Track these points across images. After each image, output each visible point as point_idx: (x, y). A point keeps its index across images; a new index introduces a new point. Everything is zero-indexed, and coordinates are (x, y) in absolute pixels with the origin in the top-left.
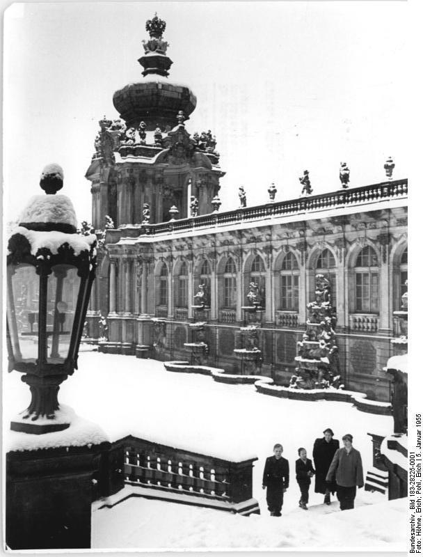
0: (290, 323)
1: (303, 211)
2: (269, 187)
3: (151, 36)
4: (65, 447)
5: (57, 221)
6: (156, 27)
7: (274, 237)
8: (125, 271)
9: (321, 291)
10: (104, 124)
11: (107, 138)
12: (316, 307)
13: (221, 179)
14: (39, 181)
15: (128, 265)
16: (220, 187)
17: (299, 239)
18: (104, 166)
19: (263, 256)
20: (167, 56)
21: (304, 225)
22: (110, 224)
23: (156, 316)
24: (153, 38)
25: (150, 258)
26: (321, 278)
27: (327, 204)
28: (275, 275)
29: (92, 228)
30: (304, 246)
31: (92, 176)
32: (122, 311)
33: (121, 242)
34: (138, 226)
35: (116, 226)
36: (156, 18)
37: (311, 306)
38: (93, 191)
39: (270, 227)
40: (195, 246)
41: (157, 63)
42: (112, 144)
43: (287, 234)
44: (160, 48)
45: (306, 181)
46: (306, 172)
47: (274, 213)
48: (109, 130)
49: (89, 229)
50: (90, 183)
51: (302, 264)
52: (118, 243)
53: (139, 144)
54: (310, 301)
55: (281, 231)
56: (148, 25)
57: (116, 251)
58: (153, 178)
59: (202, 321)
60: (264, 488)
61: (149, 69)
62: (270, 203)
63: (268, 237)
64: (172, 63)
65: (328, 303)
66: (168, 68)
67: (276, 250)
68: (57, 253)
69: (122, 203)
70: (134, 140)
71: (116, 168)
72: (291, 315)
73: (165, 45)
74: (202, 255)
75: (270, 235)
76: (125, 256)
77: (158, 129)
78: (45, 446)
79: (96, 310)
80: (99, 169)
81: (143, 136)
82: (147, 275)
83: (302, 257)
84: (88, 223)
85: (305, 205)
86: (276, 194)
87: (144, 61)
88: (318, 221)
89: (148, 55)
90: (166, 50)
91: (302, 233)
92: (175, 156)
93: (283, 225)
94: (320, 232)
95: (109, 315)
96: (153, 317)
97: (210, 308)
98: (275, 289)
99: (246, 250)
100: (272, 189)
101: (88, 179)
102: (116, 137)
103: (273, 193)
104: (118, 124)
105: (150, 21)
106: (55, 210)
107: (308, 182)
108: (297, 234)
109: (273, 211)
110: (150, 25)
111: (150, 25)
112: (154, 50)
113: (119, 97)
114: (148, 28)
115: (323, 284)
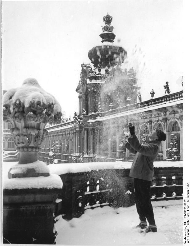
0: (160, 159)
1: (165, 102)
2: (150, 91)
3: (106, 24)
6: (108, 20)
7: (153, 116)
9: (173, 142)
10: (83, 66)
11: (84, 72)
12: (171, 151)
17: (163, 117)
18: (84, 86)
19: (148, 125)
20: (113, 33)
21: (165, 109)
22: (84, 113)
23: (103, 156)
24: (107, 25)
26: (173, 136)
27: (176, 98)
29: (78, 115)
30: (166, 120)
31: (78, 91)
32: (90, 153)
33: (89, 121)
34: (96, 114)
35: (87, 113)
37: (168, 150)
38: (80, 97)
39: (150, 111)
40: (120, 122)
41: (108, 36)
42: (86, 75)
43: (158, 114)
44: (109, 29)
45: (167, 87)
46: (167, 83)
47: (153, 104)
48: (85, 68)
49: (77, 115)
50: (78, 94)
51: (165, 129)
52: (88, 122)
53: (97, 75)
54: (168, 148)
55: (155, 113)
57: (87, 125)
59: (122, 158)
61: (104, 39)
62: (151, 99)
63: (150, 116)
64: (115, 36)
65: (176, 148)
66: (114, 39)
67: (154, 123)
69: (90, 102)
70: (96, 73)
71: (88, 86)
72: (160, 155)
73: (112, 28)
75: (151, 115)
76: (91, 128)
77: (107, 67)
79: (80, 153)
80: (82, 87)
81: (100, 71)
83: (165, 126)
84: (77, 113)
85: (166, 99)
86: (154, 95)
87: (102, 36)
88: (171, 107)
89: (104, 33)
90: (112, 30)
91: (165, 113)
93: (156, 110)
94: (172, 113)
95: (84, 155)
96: (102, 156)
97: (125, 152)
99: (141, 123)
100: (152, 92)
101: (78, 92)
102: (88, 72)
103: (152, 94)
104: (89, 65)
105: (105, 17)
107: (168, 88)
108: (162, 114)
109: (152, 103)
110: (105, 19)
112: (106, 31)
113: (90, 53)
114: (104, 20)
115: (174, 139)
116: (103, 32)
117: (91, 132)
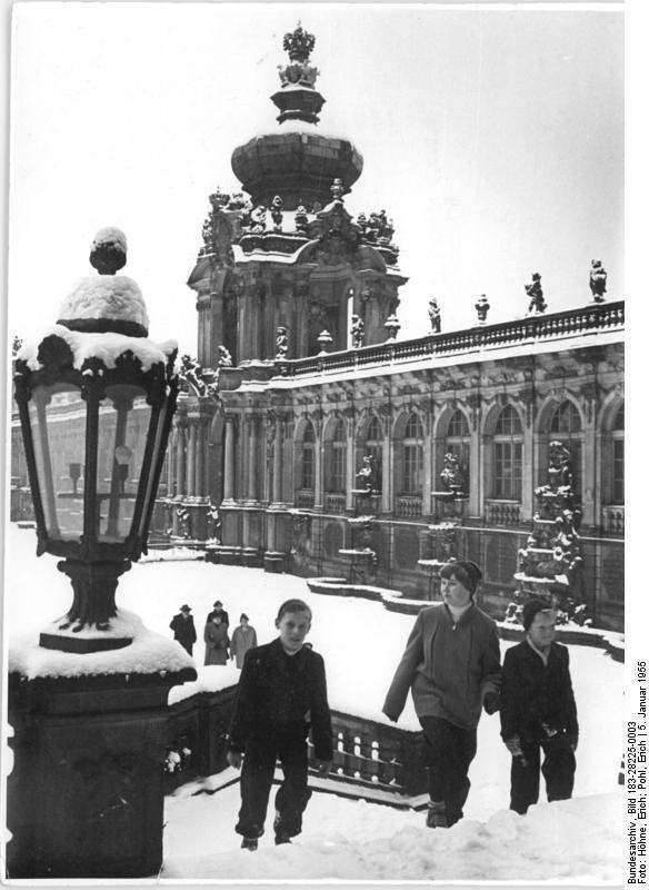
0: (508, 519)
1: (530, 339)
3: (292, 58)
4: (123, 675)
5: (115, 318)
6: (299, 45)
7: (485, 381)
8: (249, 434)
9: (557, 468)
10: (218, 200)
11: (221, 223)
12: (550, 494)
13: (401, 289)
14: (89, 255)
15: (253, 423)
16: (398, 302)
17: (523, 384)
18: (217, 267)
19: (467, 411)
20: (317, 90)
21: (531, 362)
22: (226, 360)
23: (295, 507)
24: (295, 62)
25: (288, 413)
26: (558, 447)
27: (569, 329)
28: (485, 443)
29: (198, 366)
30: (531, 395)
31: (198, 284)
32: (243, 497)
33: (243, 388)
34: (269, 363)
35: (235, 362)
36: (300, 30)
37: (542, 493)
38: (200, 306)
39: (478, 365)
40: (359, 396)
41: (300, 101)
42: (230, 233)
43: (505, 376)
44: (306, 78)
45: (535, 291)
46: (536, 277)
47: (485, 343)
48: (225, 209)
49: (193, 367)
50: (195, 294)
51: (528, 424)
52: (237, 390)
53: (271, 232)
54: (540, 485)
55: (495, 372)
56: (286, 42)
57: (235, 402)
58: (293, 285)
59: (368, 515)
60: (108, 350)
61: (287, 111)
62: (478, 325)
63: (474, 381)
64: (324, 101)
65: (568, 487)
66: (318, 110)
67: (488, 402)
68: (114, 366)
69: (246, 326)
70: (264, 226)
71: (236, 271)
72: (510, 506)
73: (314, 73)
74: (369, 409)
75: (478, 378)
76: (249, 410)
77: (301, 208)
78: (92, 671)
79: (203, 495)
80: (208, 273)
81: (278, 219)
82: (282, 441)
83: (529, 413)
84: (192, 358)
85: (534, 329)
86: (488, 312)
87: (279, 99)
88: (555, 355)
89: (287, 89)
90: (315, 80)
91: (528, 374)
92: (328, 251)
93: (499, 362)
94: (557, 373)
95: (224, 503)
96: (290, 507)
97: (381, 494)
98: (485, 464)
99: (440, 402)
100: (482, 304)
101: (192, 288)
102: (236, 221)
103: (483, 310)
104: (240, 199)
105: (289, 35)
106: (112, 300)
107: (540, 293)
108: (521, 376)
109: (483, 338)
110: (290, 41)
111: (290, 41)
112: (295, 82)
113: (240, 157)
114: (287, 46)
115: (561, 456)
116: (283, 86)
117: (246, 428)
